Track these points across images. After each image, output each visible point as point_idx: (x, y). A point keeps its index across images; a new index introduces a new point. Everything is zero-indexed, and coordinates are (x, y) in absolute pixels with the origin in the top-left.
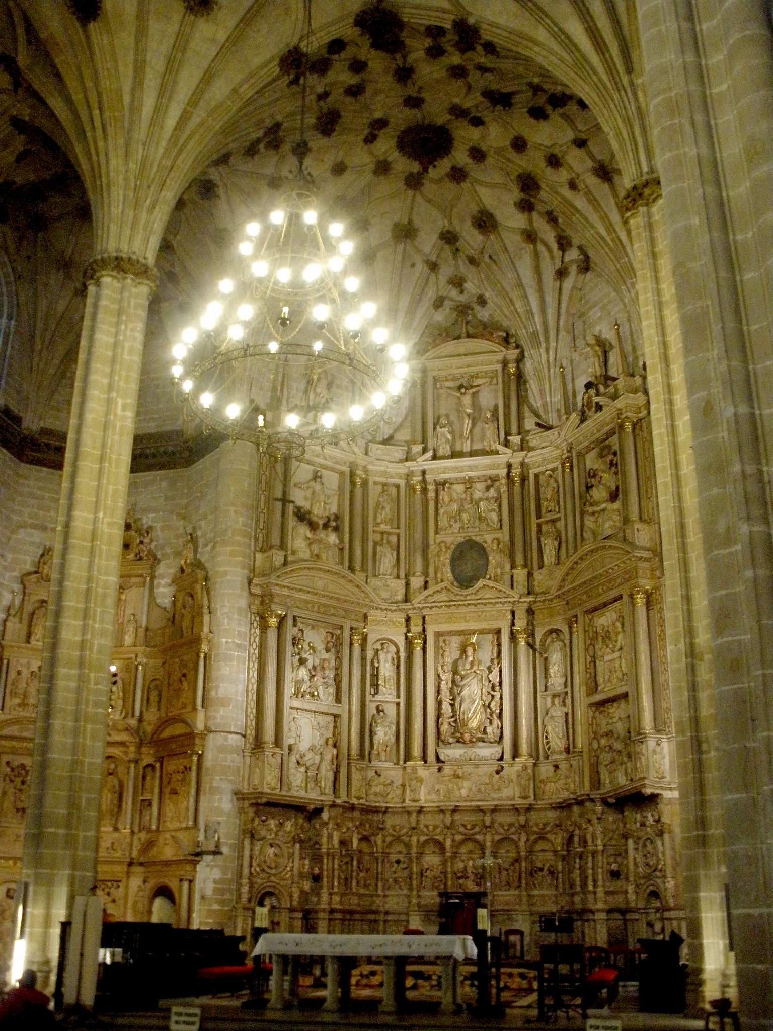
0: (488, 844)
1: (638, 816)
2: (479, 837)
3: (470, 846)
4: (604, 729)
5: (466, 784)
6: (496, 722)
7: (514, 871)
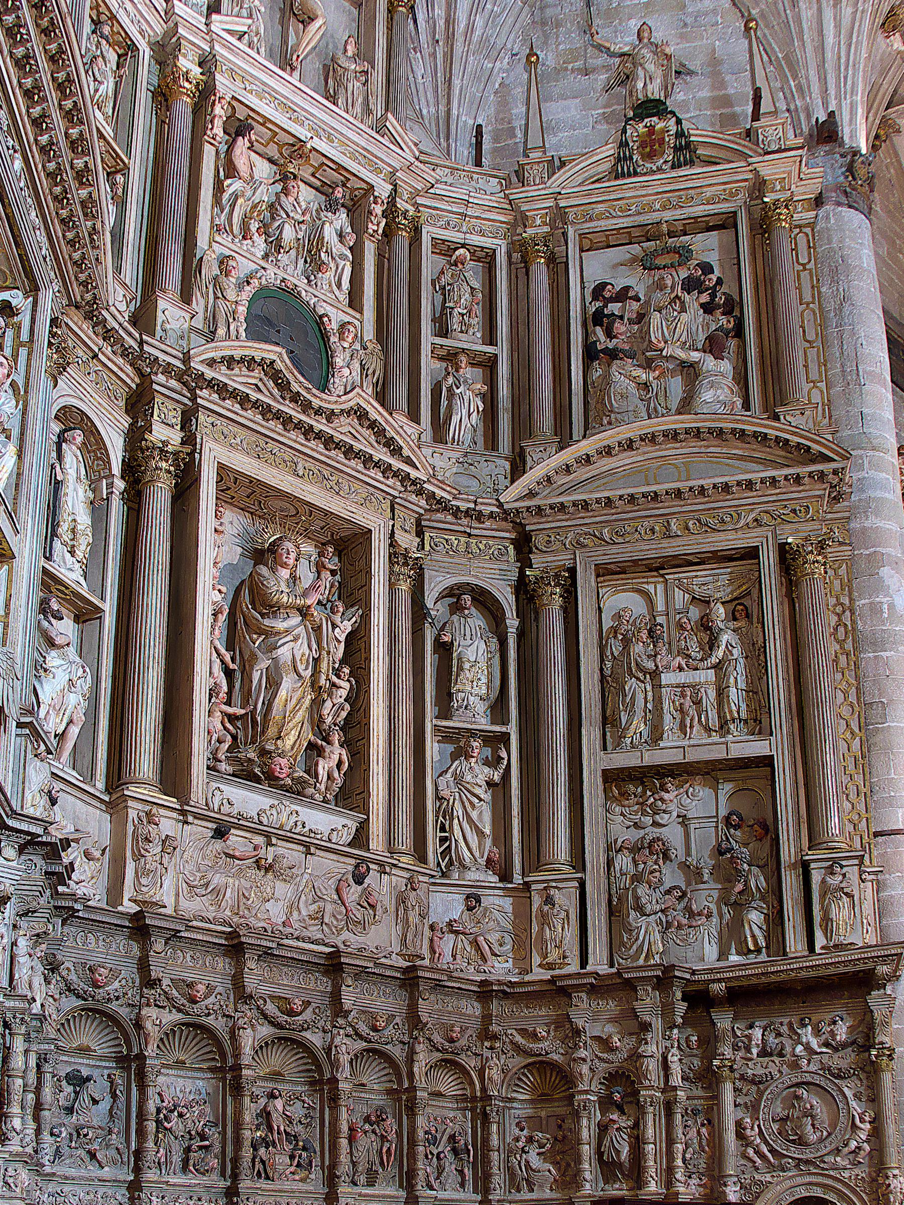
0: (344, 1059)
1: (757, 1033)
2: (315, 1039)
3: (277, 1059)
4: (626, 835)
5: (283, 890)
6: (336, 752)
7: (383, 1138)
